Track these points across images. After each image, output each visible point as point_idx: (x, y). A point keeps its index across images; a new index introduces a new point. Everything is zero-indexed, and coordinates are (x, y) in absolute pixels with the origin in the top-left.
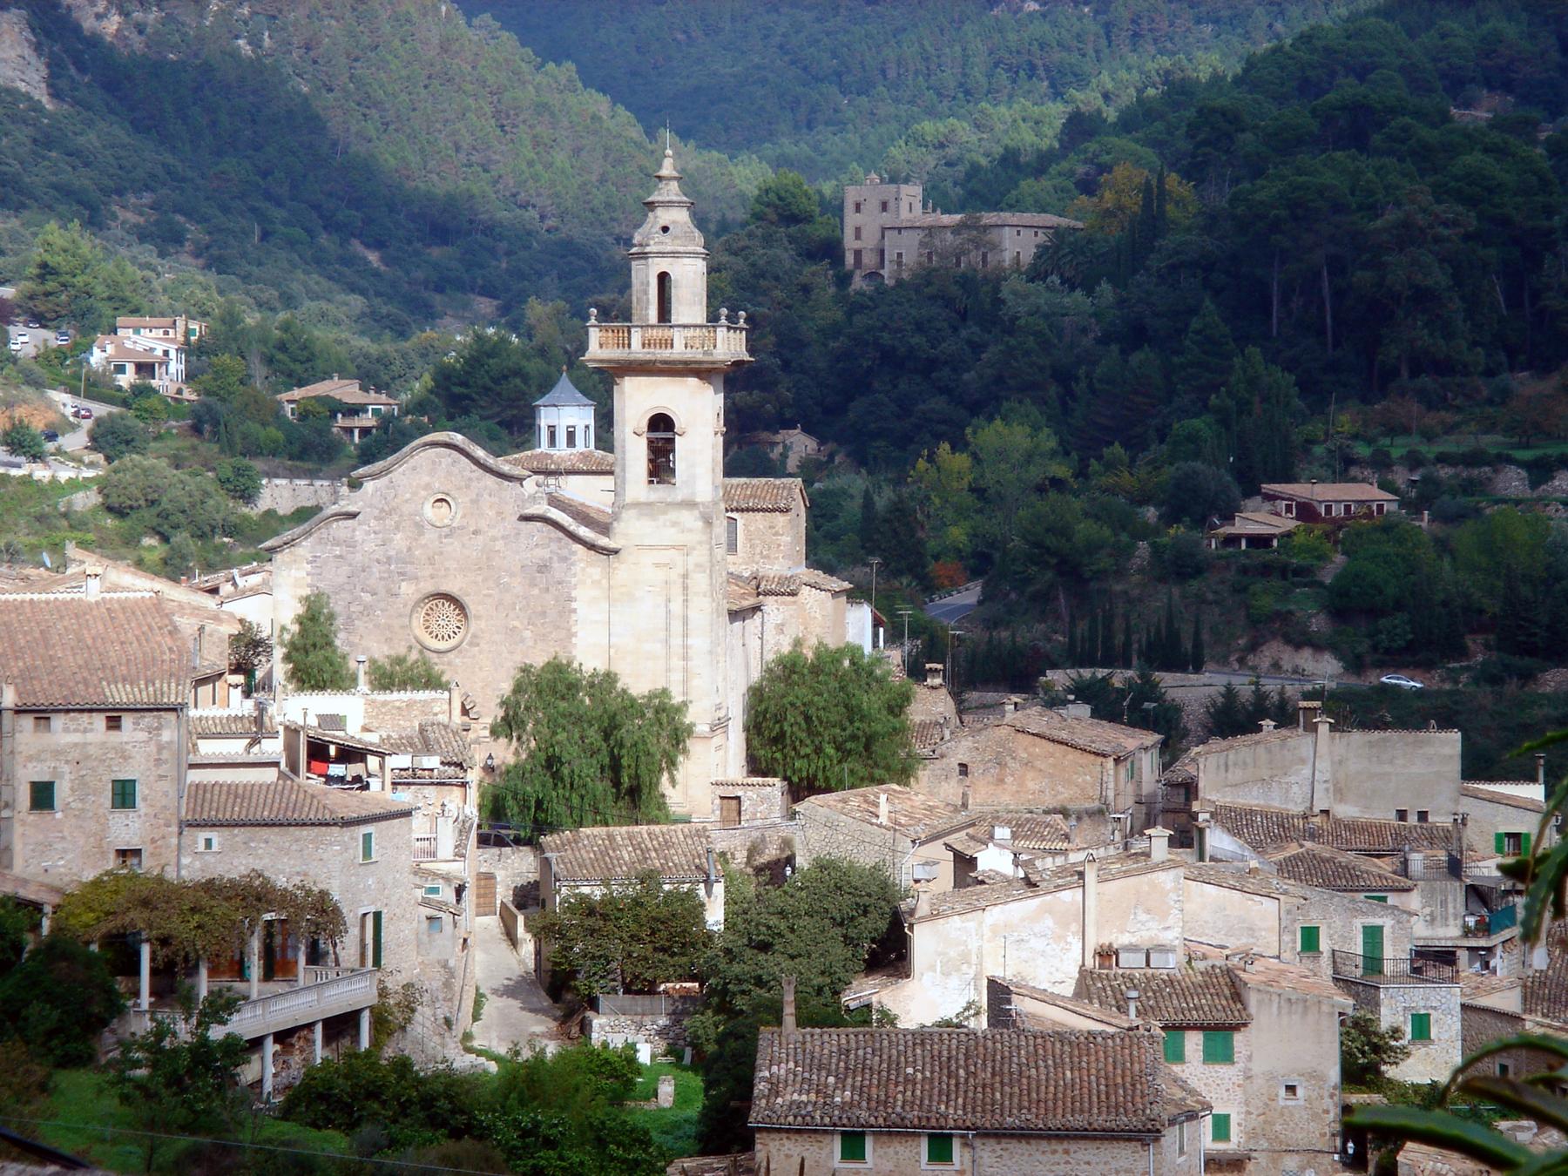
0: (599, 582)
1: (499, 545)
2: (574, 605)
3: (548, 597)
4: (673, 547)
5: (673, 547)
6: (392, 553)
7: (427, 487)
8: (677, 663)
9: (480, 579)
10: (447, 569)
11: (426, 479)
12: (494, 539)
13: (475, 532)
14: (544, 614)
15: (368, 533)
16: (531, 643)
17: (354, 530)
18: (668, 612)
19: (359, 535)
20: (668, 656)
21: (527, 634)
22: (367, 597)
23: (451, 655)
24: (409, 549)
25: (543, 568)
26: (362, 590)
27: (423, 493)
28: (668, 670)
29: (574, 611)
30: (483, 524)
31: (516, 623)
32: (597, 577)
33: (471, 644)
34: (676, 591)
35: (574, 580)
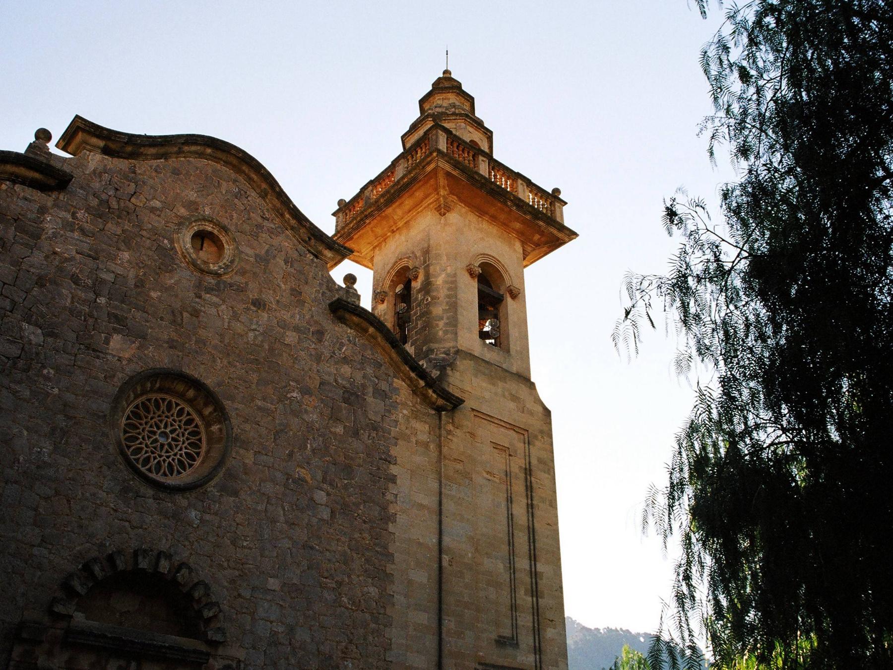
0: (426, 445)
1: (291, 337)
2: (394, 470)
3: (356, 444)
4: (512, 427)
5: (512, 427)
6: (110, 277)
7: (192, 206)
8: (525, 599)
9: (254, 377)
10: (202, 342)
11: (193, 196)
12: (283, 325)
13: (259, 304)
14: (348, 470)
15: (69, 226)
16: (326, 514)
17: (43, 210)
18: (510, 517)
19: (50, 224)
20: (513, 590)
21: (321, 496)
22: (33, 334)
23: (182, 500)
24: (140, 283)
25: (352, 396)
26: (28, 319)
27: (183, 211)
28: (514, 607)
29: (393, 479)
30: (269, 297)
31: (303, 472)
32: (424, 437)
33: (223, 489)
34: (519, 487)
35: (394, 431)
